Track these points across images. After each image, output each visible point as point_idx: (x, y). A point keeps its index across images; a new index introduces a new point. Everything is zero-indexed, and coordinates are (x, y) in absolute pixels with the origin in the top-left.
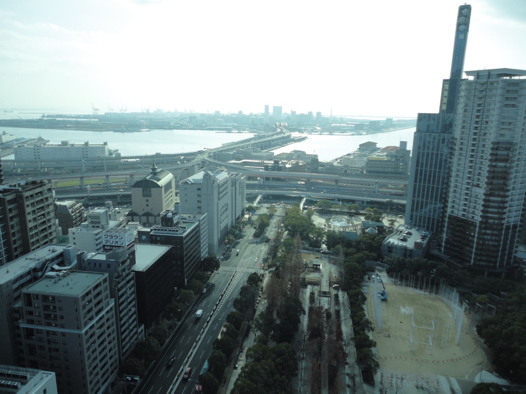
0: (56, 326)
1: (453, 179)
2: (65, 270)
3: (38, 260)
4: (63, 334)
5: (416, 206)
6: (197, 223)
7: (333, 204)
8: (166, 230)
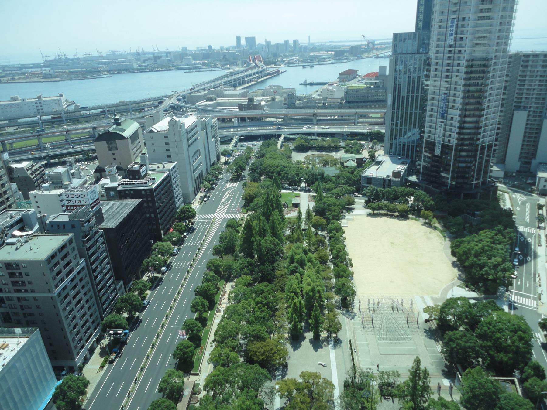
0: (26, 291)
1: (429, 102)
4: (35, 299)
5: (395, 134)
6: (168, 172)
7: (312, 140)
8: (134, 184)
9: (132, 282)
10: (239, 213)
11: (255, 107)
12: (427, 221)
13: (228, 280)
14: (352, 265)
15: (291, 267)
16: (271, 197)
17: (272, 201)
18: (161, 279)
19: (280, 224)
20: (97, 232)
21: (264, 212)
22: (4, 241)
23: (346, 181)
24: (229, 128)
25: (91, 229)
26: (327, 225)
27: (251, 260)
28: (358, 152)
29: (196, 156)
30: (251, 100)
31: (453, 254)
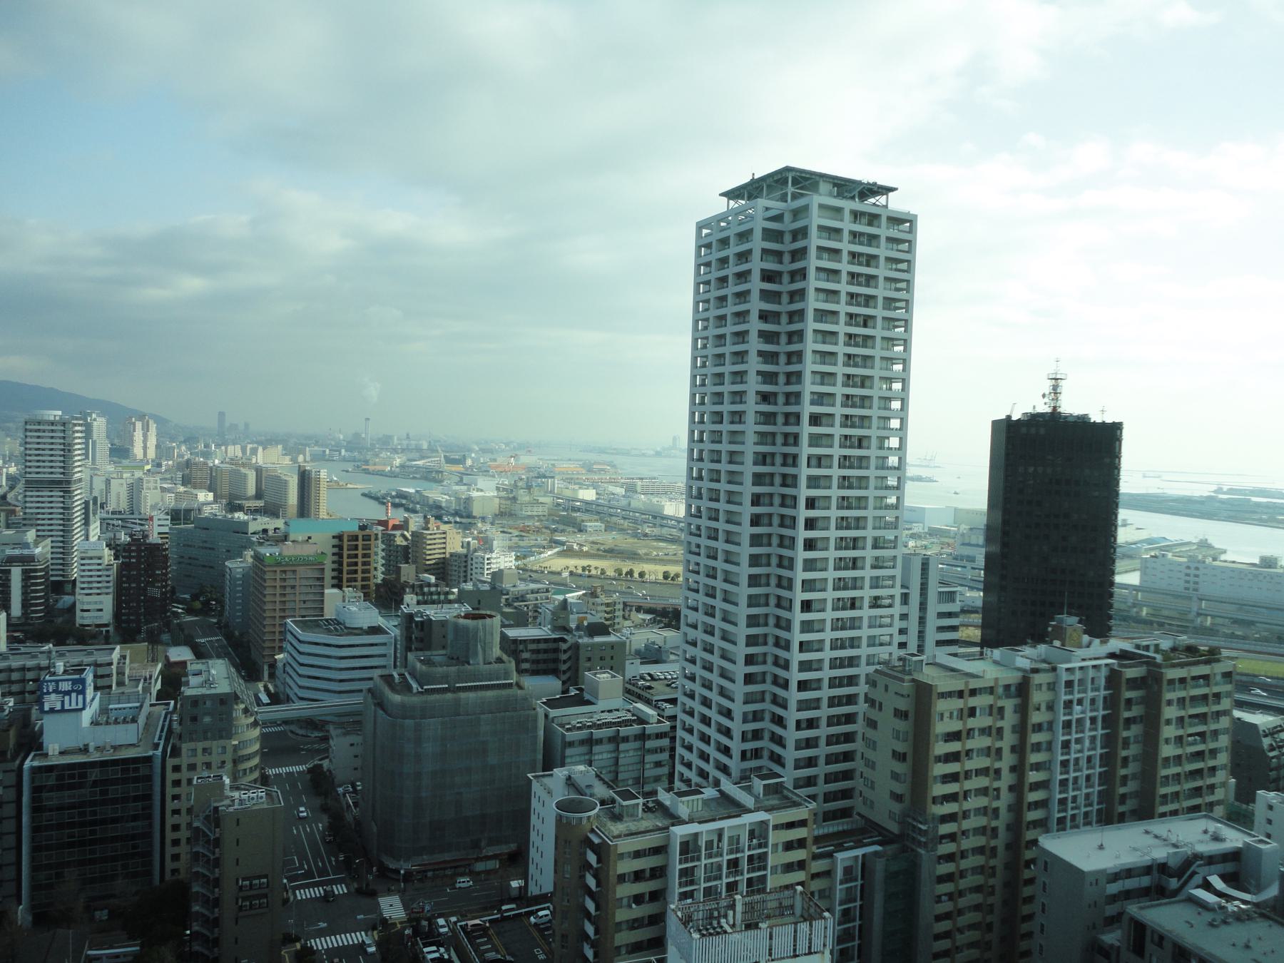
2: (1244, 902)
3: (1175, 846)
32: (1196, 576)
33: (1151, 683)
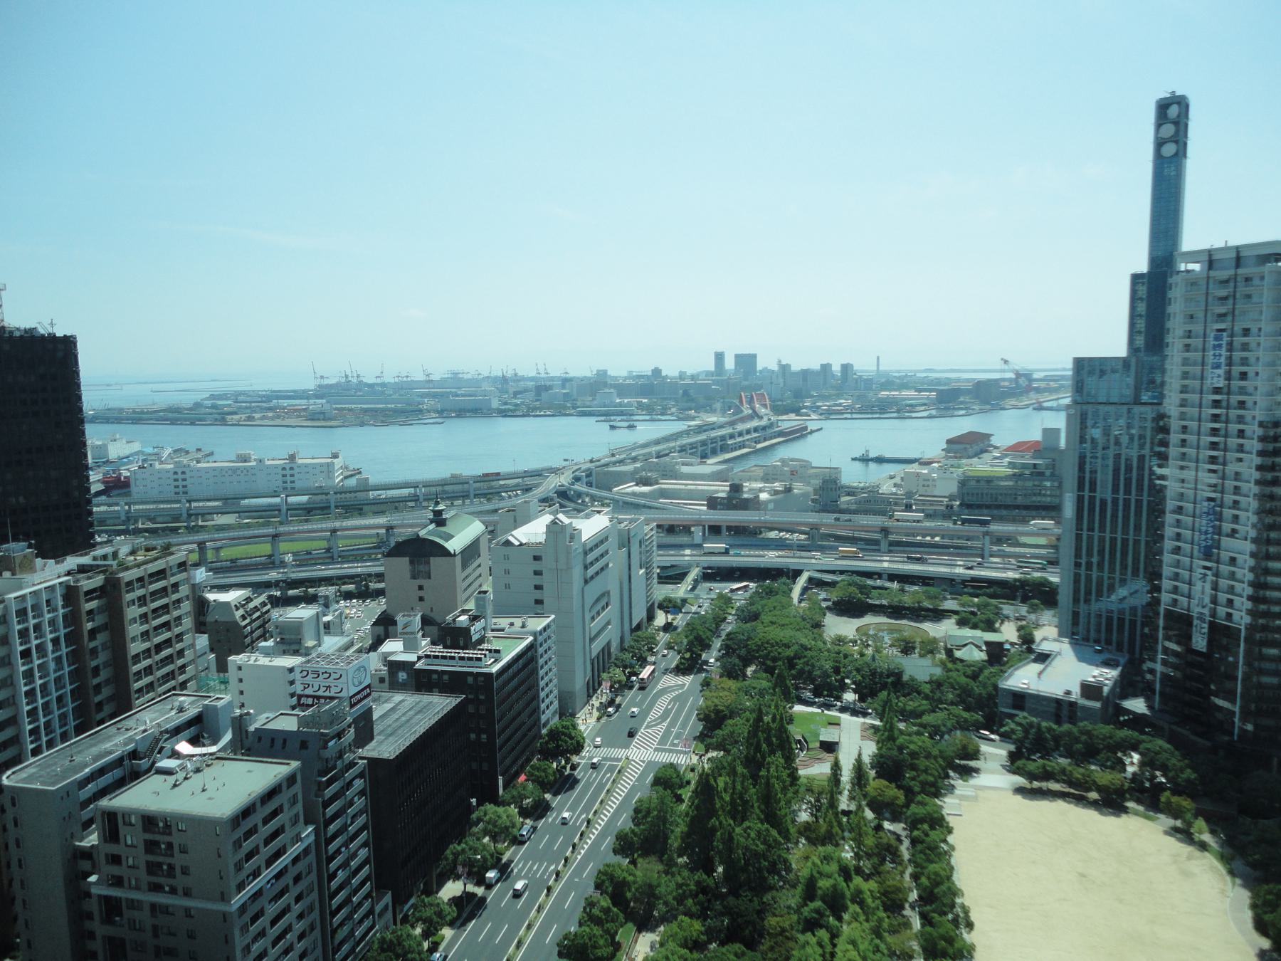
0: (173, 891)
1: (1170, 518)
4: (188, 912)
5: (1084, 590)
6: (531, 638)
8: (453, 658)
9: (412, 901)
10: (685, 753)
11: (745, 505)
12: (1179, 823)
13: (644, 925)
14: (970, 926)
15: (806, 911)
16: (767, 719)
17: (769, 730)
18: (483, 900)
19: (784, 789)
20: (352, 764)
21: (746, 757)
22: (154, 763)
23: (959, 696)
24: (682, 547)
25: (340, 755)
26: (907, 805)
27: (705, 877)
28: (989, 626)
29: (599, 607)
30: (736, 488)
31: (1261, 926)
32: (184, 480)
33: (111, 591)
